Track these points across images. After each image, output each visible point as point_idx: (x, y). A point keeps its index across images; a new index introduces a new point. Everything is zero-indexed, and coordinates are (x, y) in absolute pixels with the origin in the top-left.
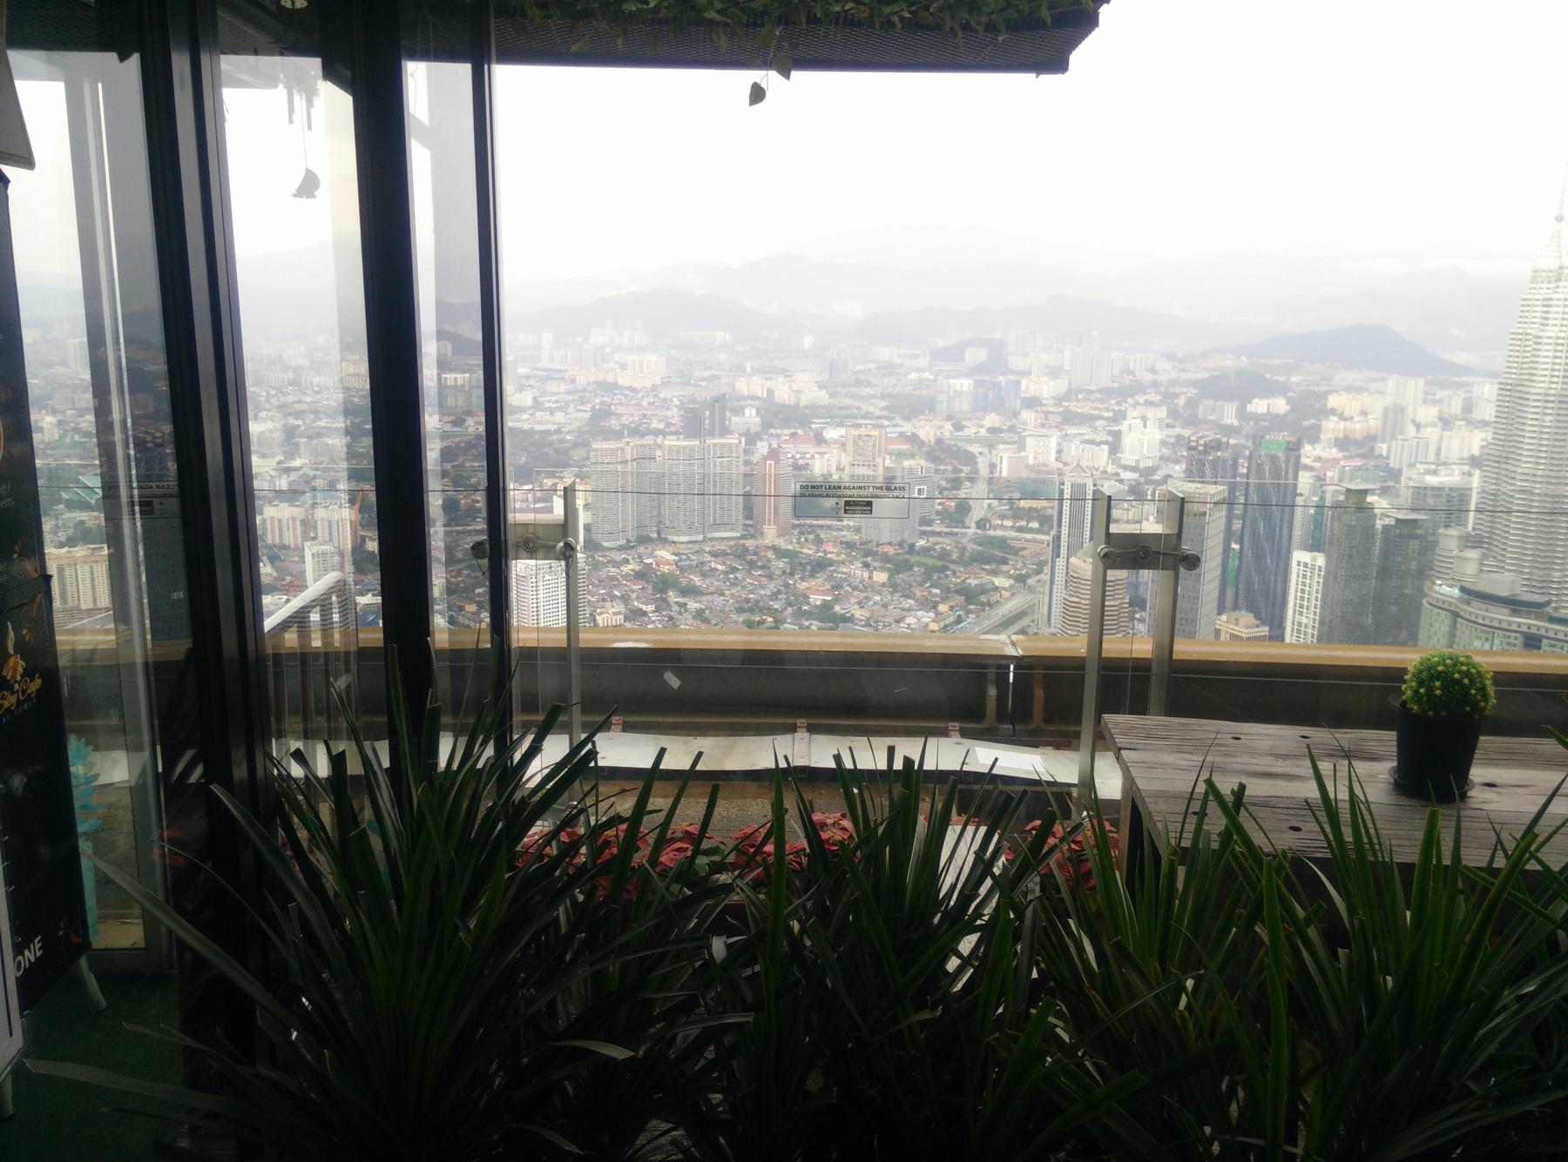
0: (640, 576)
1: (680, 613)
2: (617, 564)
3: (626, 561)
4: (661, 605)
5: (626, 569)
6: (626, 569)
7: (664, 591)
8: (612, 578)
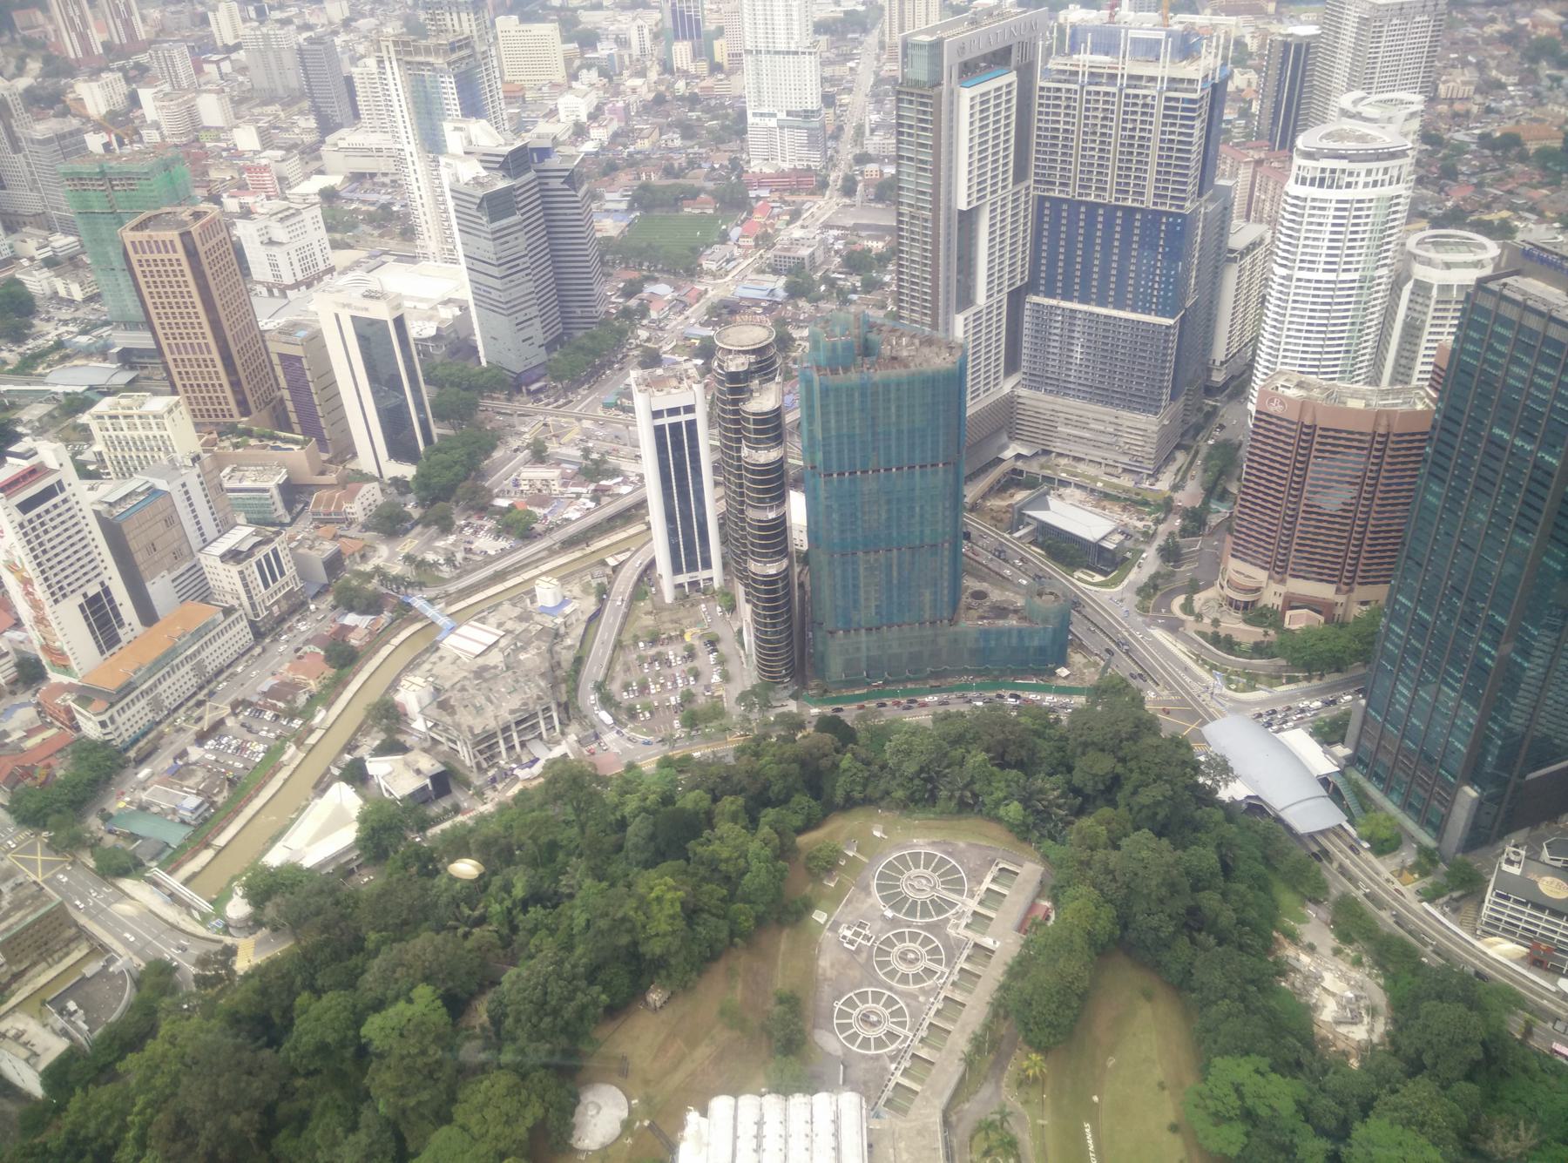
0: (1508, 39)
1: (1551, 89)
2: (1479, 24)
3: (1493, 20)
4: (1528, 79)
5: (1489, 30)
6: (1489, 30)
7: (1534, 60)
8: (1468, 41)
